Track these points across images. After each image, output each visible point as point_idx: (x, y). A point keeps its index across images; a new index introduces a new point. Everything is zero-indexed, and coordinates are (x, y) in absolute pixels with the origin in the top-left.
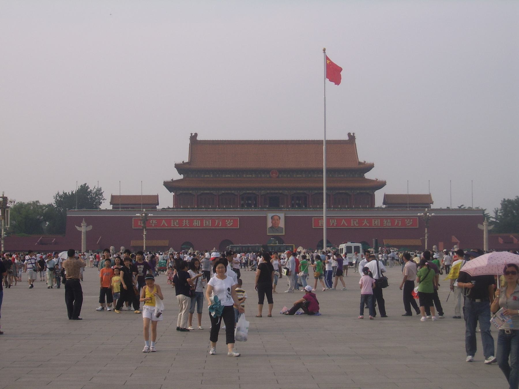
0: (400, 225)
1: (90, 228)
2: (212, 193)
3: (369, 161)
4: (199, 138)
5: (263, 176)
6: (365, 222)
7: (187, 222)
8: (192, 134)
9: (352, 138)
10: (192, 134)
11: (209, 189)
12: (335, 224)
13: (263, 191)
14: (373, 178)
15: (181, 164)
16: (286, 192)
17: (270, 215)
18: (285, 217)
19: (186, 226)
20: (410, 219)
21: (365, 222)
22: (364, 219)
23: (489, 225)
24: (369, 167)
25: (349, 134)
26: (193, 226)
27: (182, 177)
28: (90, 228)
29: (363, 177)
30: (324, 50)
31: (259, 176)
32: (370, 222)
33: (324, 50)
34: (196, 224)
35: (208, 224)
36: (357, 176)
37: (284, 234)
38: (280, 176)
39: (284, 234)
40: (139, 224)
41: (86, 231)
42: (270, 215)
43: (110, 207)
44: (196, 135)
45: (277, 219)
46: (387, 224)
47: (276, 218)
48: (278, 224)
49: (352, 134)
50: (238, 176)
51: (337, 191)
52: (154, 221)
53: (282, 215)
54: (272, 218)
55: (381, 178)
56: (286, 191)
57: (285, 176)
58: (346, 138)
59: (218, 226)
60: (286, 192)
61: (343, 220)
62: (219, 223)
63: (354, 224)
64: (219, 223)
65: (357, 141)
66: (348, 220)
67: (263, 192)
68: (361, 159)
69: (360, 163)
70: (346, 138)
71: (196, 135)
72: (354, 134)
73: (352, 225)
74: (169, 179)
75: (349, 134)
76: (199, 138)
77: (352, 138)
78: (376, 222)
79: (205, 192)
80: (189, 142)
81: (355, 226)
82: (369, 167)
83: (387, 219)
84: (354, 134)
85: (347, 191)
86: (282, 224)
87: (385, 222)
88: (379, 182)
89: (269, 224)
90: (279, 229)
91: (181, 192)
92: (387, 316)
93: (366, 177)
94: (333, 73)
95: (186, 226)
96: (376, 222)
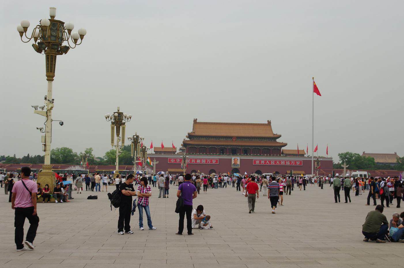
0: (294, 164)
1: (158, 162)
2: (205, 147)
3: (279, 134)
4: (198, 121)
5: (229, 139)
6: (278, 162)
7: (194, 160)
8: (194, 119)
9: (269, 123)
10: (194, 119)
11: (204, 145)
12: (264, 163)
13: (229, 147)
14: (281, 142)
15: (191, 133)
16: (240, 147)
18: (241, 159)
19: (193, 162)
20: (299, 161)
21: (278, 162)
22: (277, 161)
23: (347, 165)
24: (279, 137)
25: (268, 121)
26: (197, 163)
27: (188, 139)
28: (158, 162)
29: (275, 141)
30: (313, 78)
31: (227, 139)
32: (280, 163)
33: (313, 78)
34: (198, 161)
35: (204, 162)
36: (273, 140)
37: (239, 167)
38: (237, 140)
39: (239, 167)
40: (171, 161)
41: (156, 164)
42: (233, 158)
43: (154, 153)
44: (196, 119)
45: (236, 160)
46: (288, 163)
49: (269, 121)
50: (217, 139)
51: (264, 148)
52: (178, 160)
53: (239, 158)
54: (234, 159)
55: (285, 142)
57: (239, 140)
58: (267, 123)
59: (208, 163)
61: (267, 161)
62: (209, 162)
63: (273, 163)
64: (209, 162)
65: (271, 124)
66: (270, 162)
67: (229, 147)
68: (275, 133)
69: (274, 135)
70: (267, 123)
71: (196, 119)
72: (270, 121)
73: (272, 164)
75: (268, 121)
76: (198, 121)
77: (269, 123)
78: (283, 163)
79: (202, 146)
80: (193, 123)
81: (273, 164)
82: (279, 137)
83: (288, 161)
84: (270, 121)
85: (268, 148)
86: (239, 163)
87: (287, 162)
88: (283, 144)
89: (233, 163)
90: (237, 165)
91: (191, 146)
92: (389, 207)
93: (277, 141)
94: (316, 90)
95: (193, 162)
96: (283, 163)
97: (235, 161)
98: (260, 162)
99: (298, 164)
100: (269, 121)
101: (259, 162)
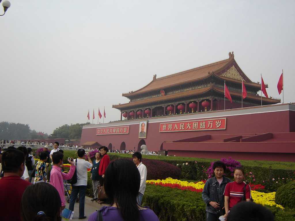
10: (154, 76)
13: (153, 106)
17: (141, 123)
18: (148, 124)
32: (191, 126)
37: (145, 138)
47: (143, 125)
48: (144, 130)
49: (232, 53)
53: (146, 123)
56: (163, 105)
60: (163, 105)
72: (233, 52)
74: (117, 104)
78: (195, 125)
89: (140, 131)
96: (195, 125)
97: (142, 128)
98: (167, 125)
99: (218, 126)
100: (232, 53)
101: (166, 126)
